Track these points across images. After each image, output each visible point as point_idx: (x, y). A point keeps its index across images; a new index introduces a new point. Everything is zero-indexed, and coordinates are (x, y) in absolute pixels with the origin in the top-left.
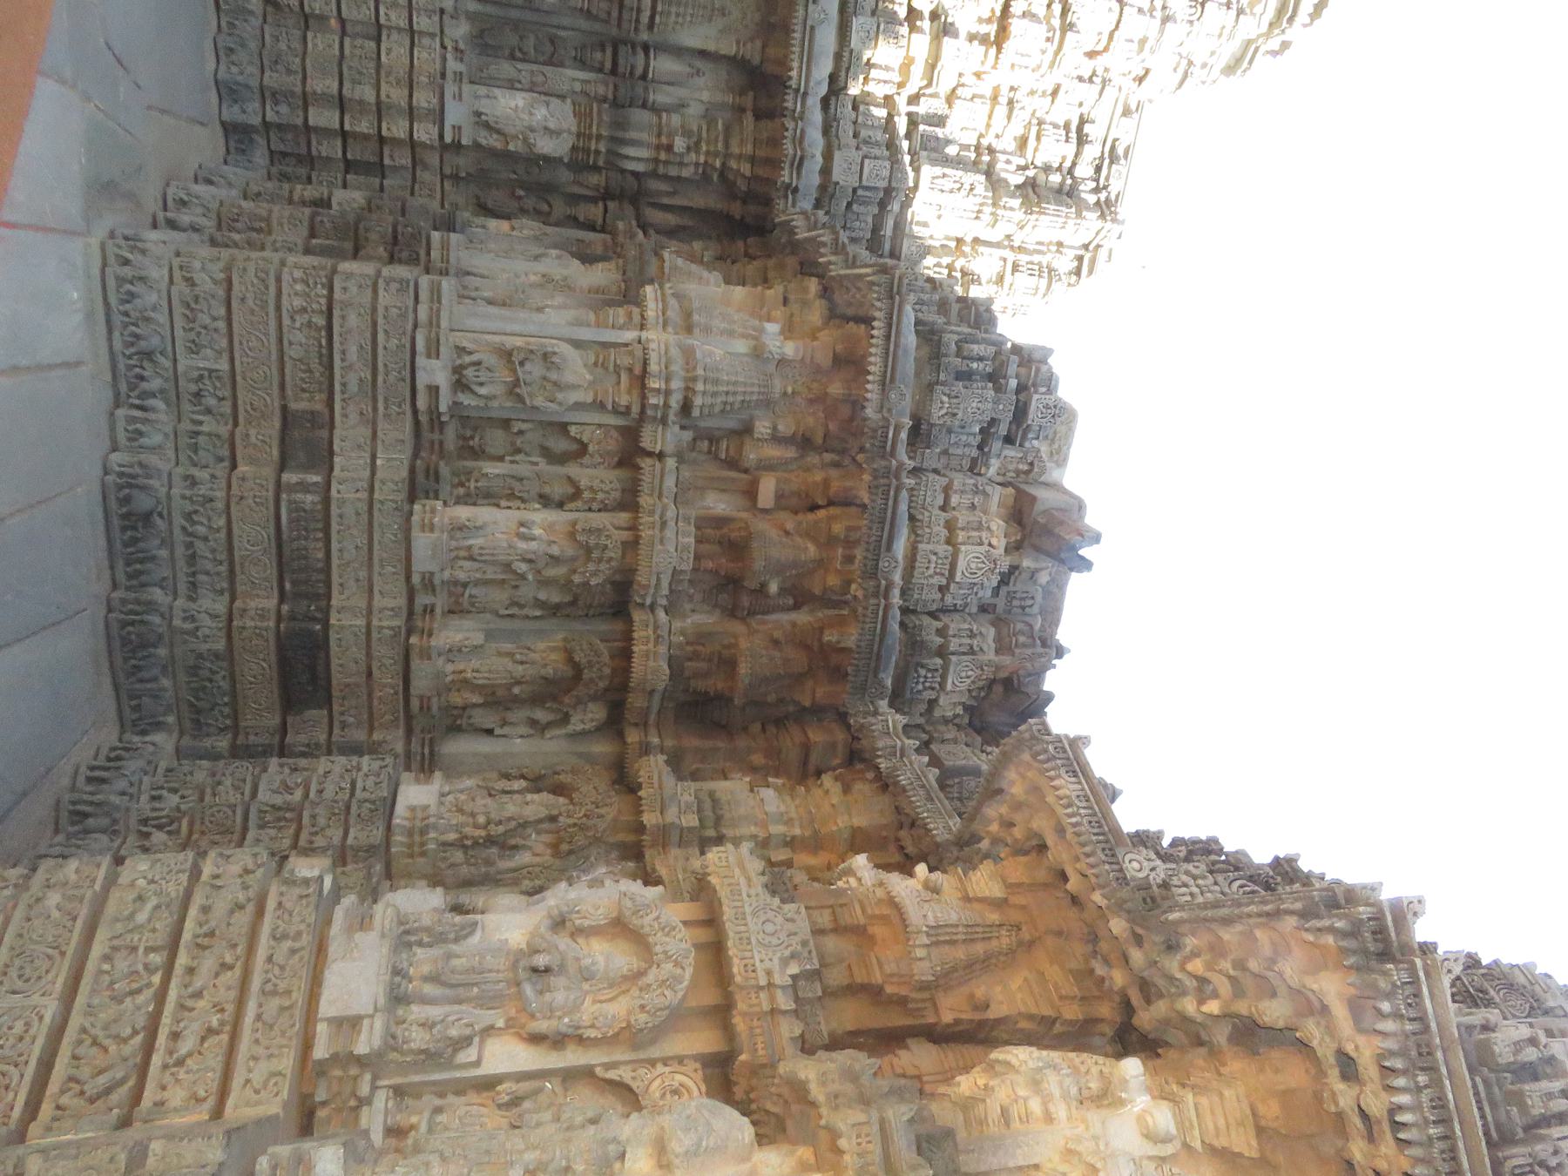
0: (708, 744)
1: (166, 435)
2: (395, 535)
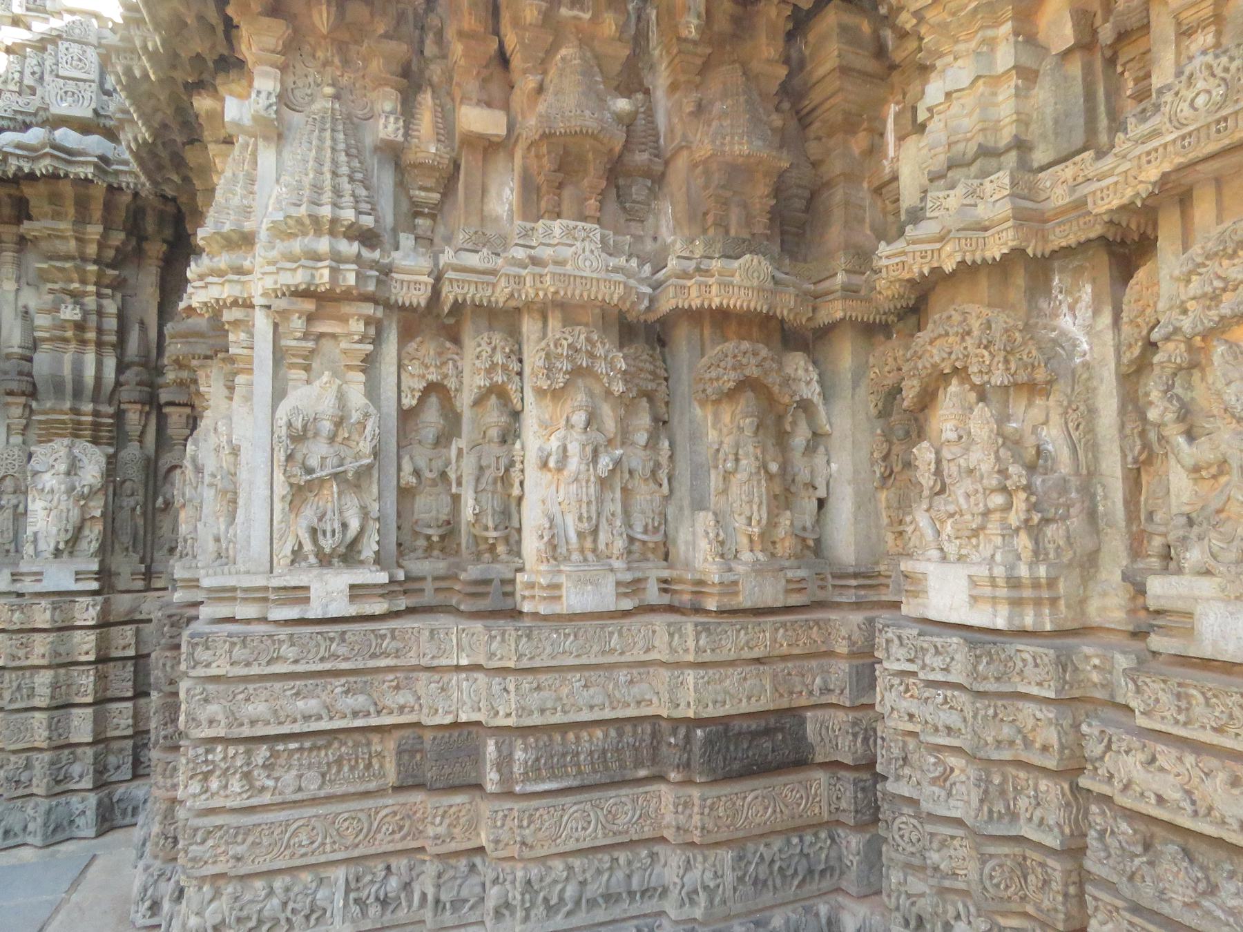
0: (838, 215)
2: (567, 636)
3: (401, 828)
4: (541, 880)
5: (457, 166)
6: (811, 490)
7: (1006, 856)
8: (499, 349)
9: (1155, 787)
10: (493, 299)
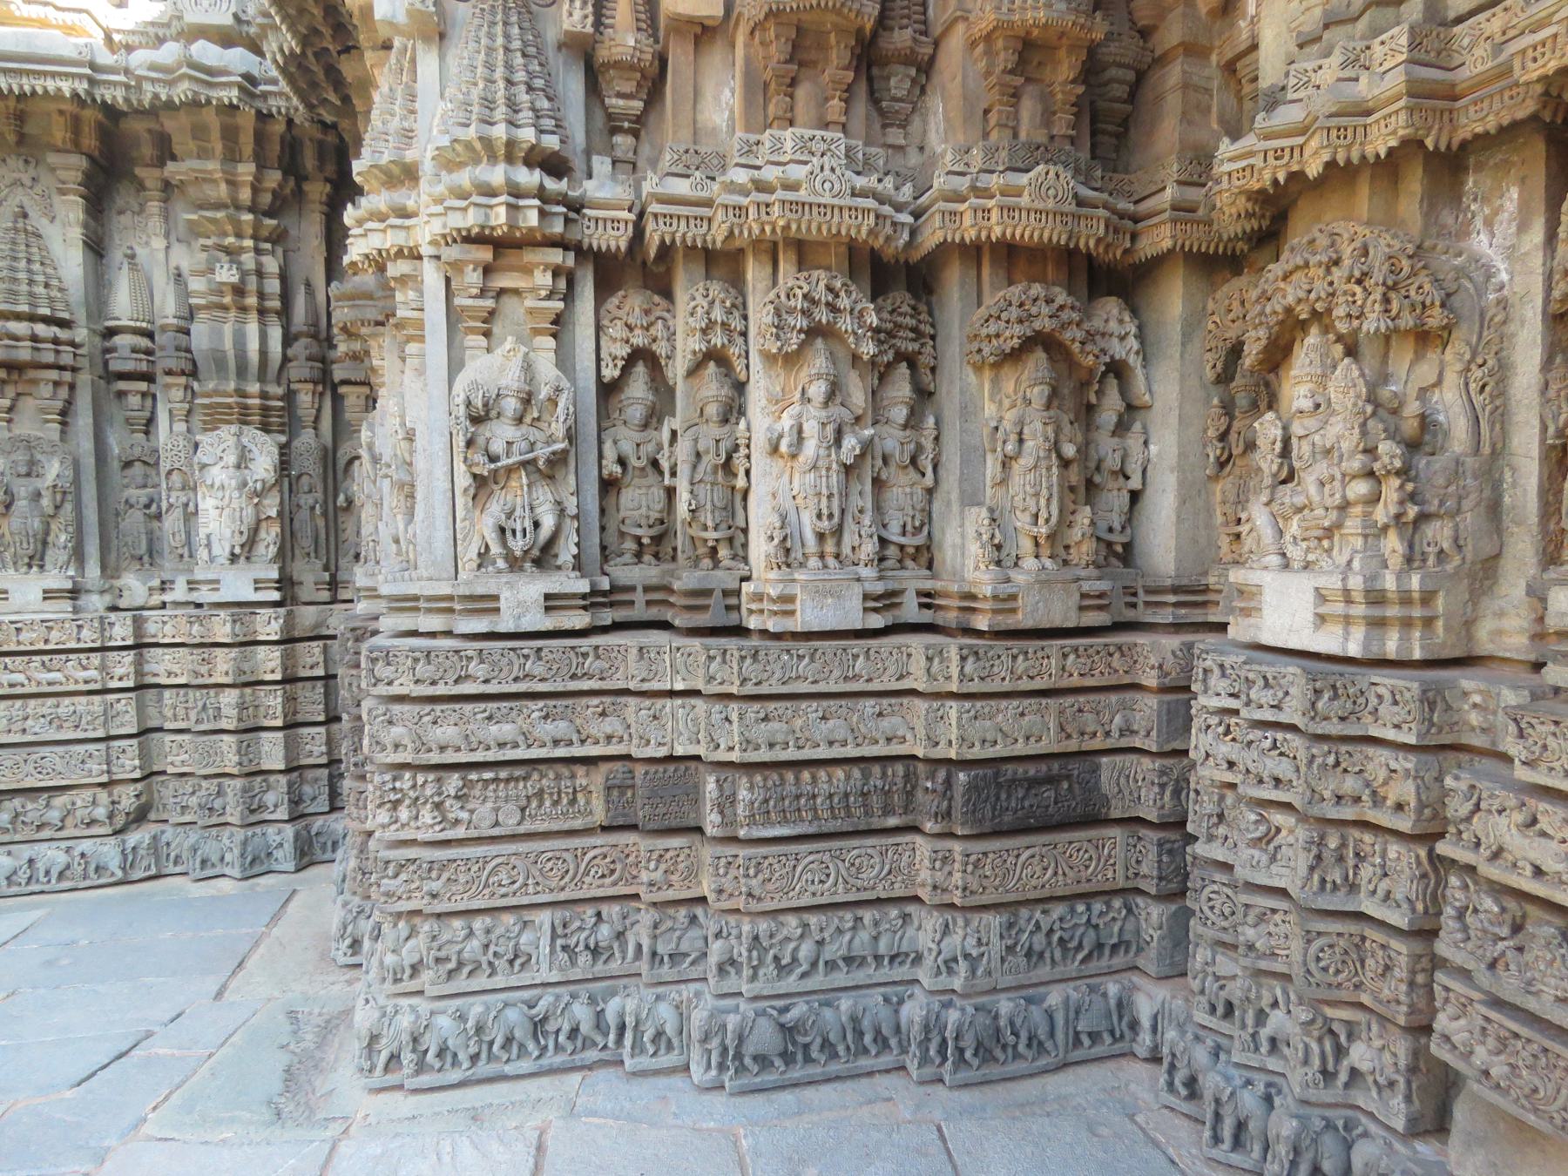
0: (1173, 103)
1: (658, 998)
2: (801, 658)
3: (613, 872)
4: (771, 936)
5: (662, 60)
6: (1121, 479)
7: (1339, 934)
8: (717, 302)
9: (1534, 855)
10: (709, 238)
